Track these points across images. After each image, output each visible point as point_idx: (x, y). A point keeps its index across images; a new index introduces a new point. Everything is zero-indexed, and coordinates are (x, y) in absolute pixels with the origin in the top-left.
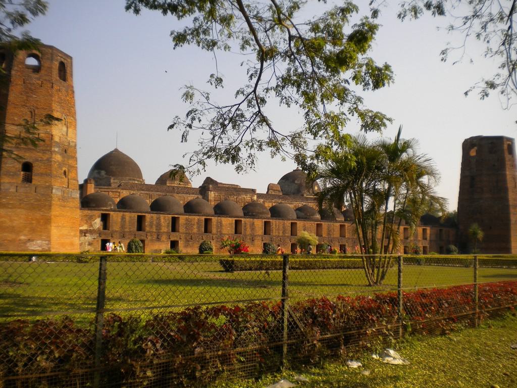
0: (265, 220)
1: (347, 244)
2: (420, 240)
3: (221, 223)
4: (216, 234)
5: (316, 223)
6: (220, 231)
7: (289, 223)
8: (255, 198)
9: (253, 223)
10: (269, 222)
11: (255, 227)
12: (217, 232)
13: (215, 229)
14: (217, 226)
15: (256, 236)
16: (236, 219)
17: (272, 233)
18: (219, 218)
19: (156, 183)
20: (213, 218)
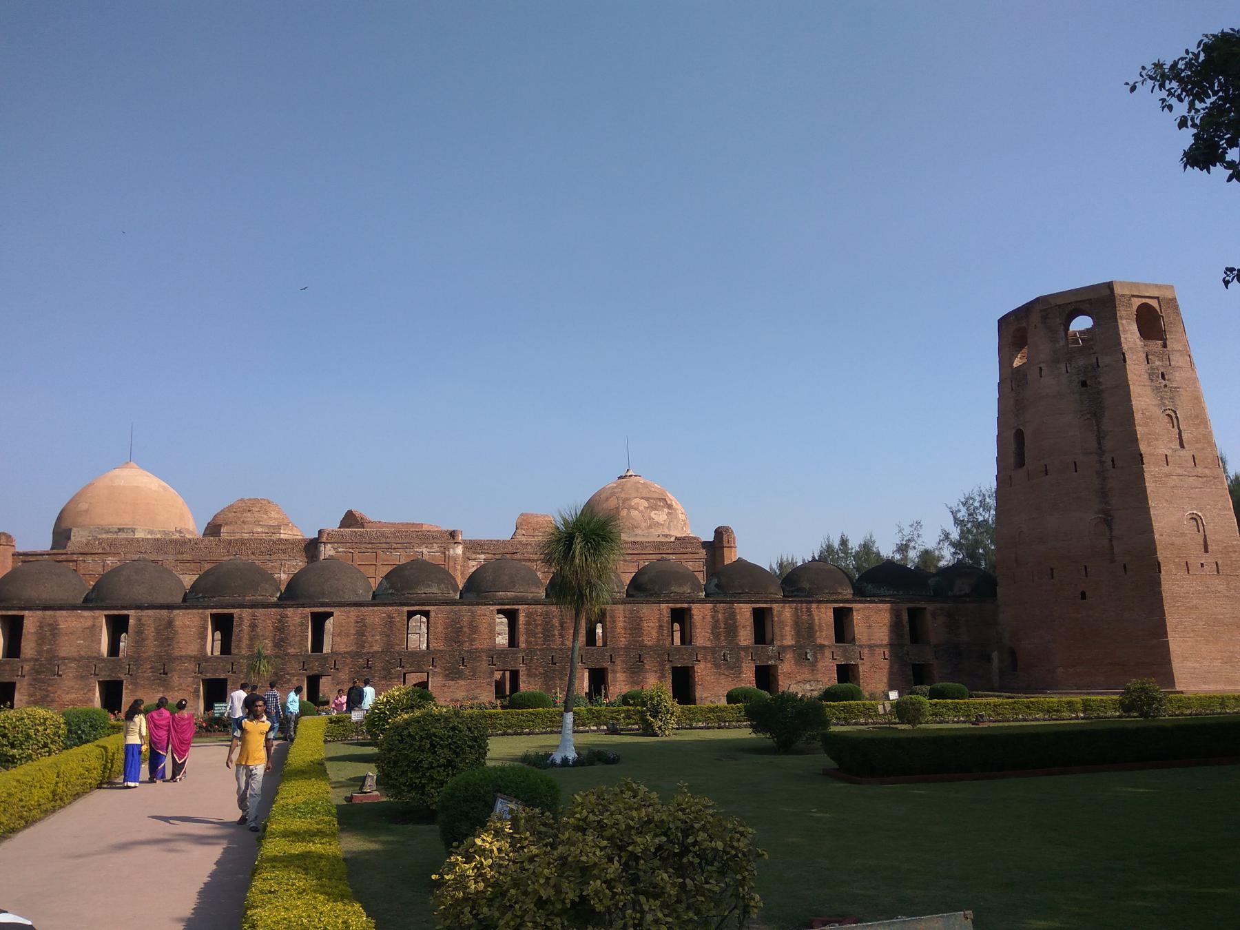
0: (215, 611)
1: (522, 668)
2: (822, 647)
3: (54, 628)
4: (37, 660)
5: (406, 609)
6: (49, 651)
7: (304, 617)
8: (459, 550)
9: (170, 624)
10: (232, 615)
11: (176, 633)
12: (40, 652)
13: (33, 645)
14: (41, 639)
15: (176, 658)
16: (107, 612)
17: (238, 647)
18: (48, 613)
19: (204, 535)
20: (26, 613)
